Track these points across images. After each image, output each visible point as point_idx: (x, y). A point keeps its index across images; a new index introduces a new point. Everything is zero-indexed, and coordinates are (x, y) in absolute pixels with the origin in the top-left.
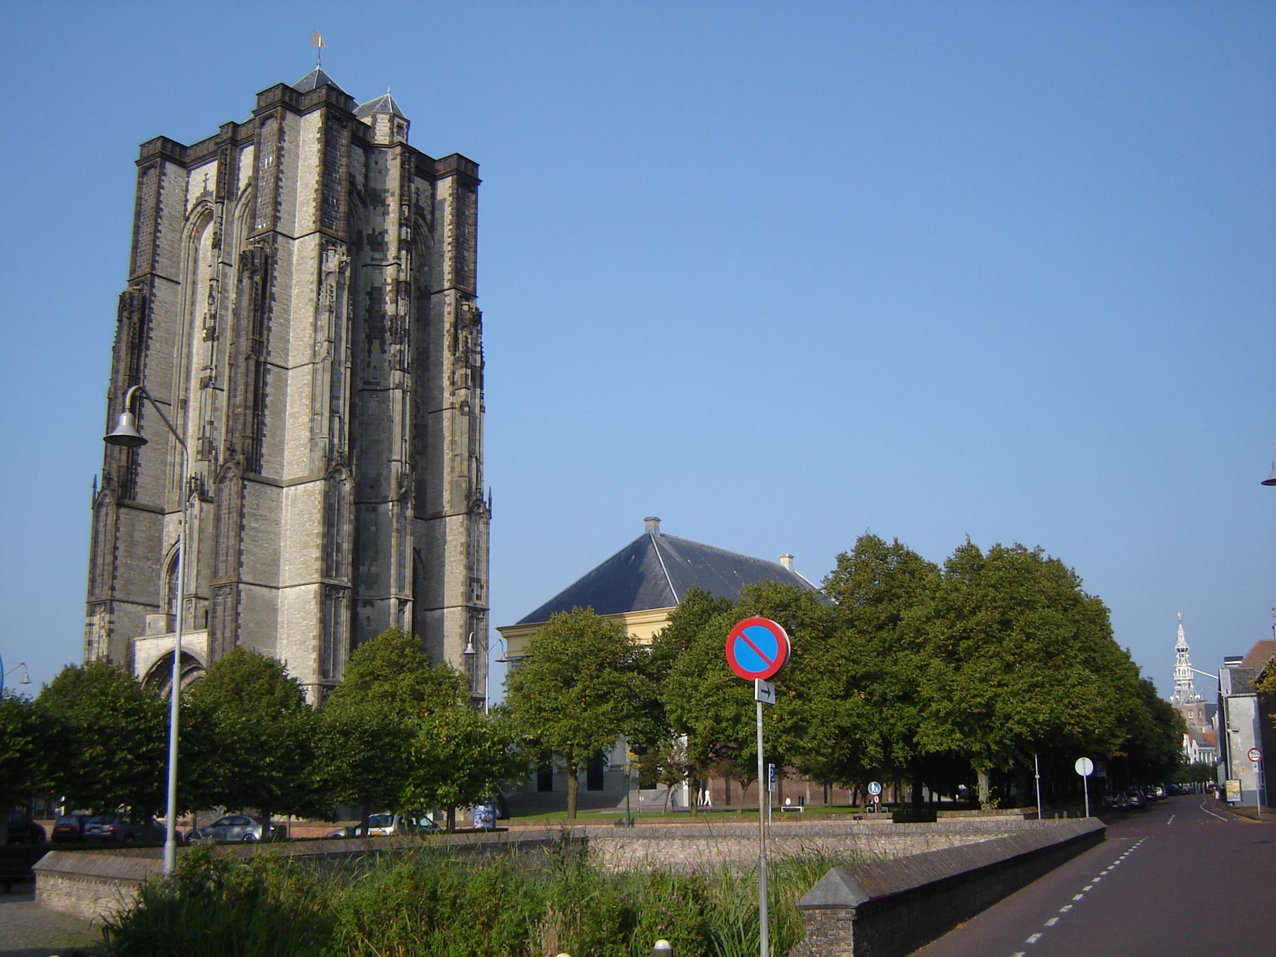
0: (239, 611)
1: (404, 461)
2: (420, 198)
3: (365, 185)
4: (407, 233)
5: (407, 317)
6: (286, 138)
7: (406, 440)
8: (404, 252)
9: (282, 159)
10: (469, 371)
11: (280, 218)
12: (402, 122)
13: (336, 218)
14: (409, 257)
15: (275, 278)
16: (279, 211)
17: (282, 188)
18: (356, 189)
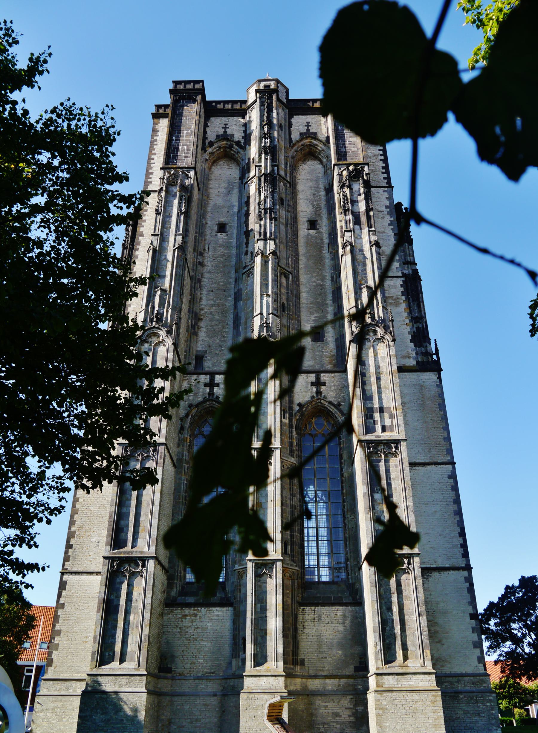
0: (77, 496)
1: (265, 314)
2: (310, 127)
3: (243, 137)
4: (265, 143)
5: (268, 200)
6: (159, 133)
7: (268, 295)
8: (263, 156)
9: (155, 147)
10: (350, 217)
11: (151, 182)
12: (268, 83)
13: (185, 157)
14: (269, 157)
15: (145, 221)
16: (151, 178)
17: (154, 163)
18: (233, 141)
